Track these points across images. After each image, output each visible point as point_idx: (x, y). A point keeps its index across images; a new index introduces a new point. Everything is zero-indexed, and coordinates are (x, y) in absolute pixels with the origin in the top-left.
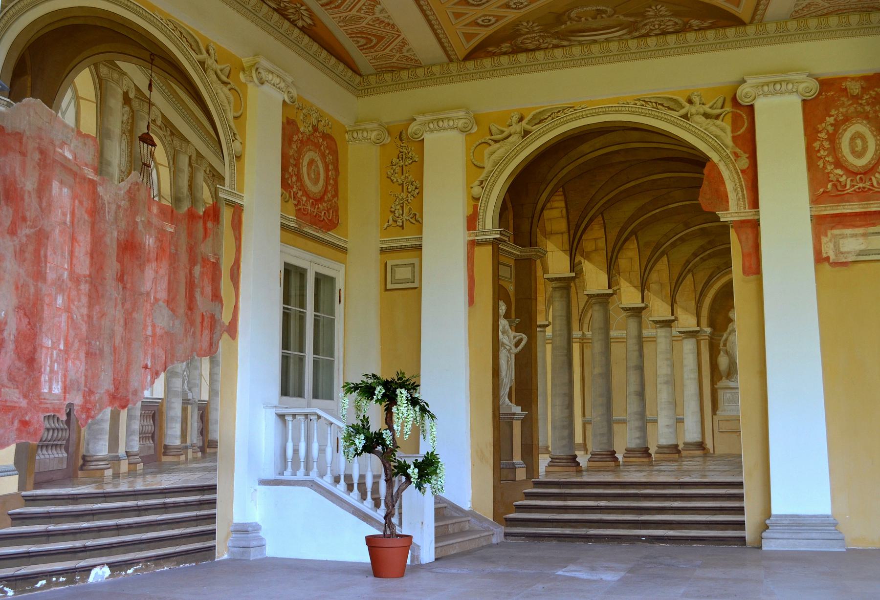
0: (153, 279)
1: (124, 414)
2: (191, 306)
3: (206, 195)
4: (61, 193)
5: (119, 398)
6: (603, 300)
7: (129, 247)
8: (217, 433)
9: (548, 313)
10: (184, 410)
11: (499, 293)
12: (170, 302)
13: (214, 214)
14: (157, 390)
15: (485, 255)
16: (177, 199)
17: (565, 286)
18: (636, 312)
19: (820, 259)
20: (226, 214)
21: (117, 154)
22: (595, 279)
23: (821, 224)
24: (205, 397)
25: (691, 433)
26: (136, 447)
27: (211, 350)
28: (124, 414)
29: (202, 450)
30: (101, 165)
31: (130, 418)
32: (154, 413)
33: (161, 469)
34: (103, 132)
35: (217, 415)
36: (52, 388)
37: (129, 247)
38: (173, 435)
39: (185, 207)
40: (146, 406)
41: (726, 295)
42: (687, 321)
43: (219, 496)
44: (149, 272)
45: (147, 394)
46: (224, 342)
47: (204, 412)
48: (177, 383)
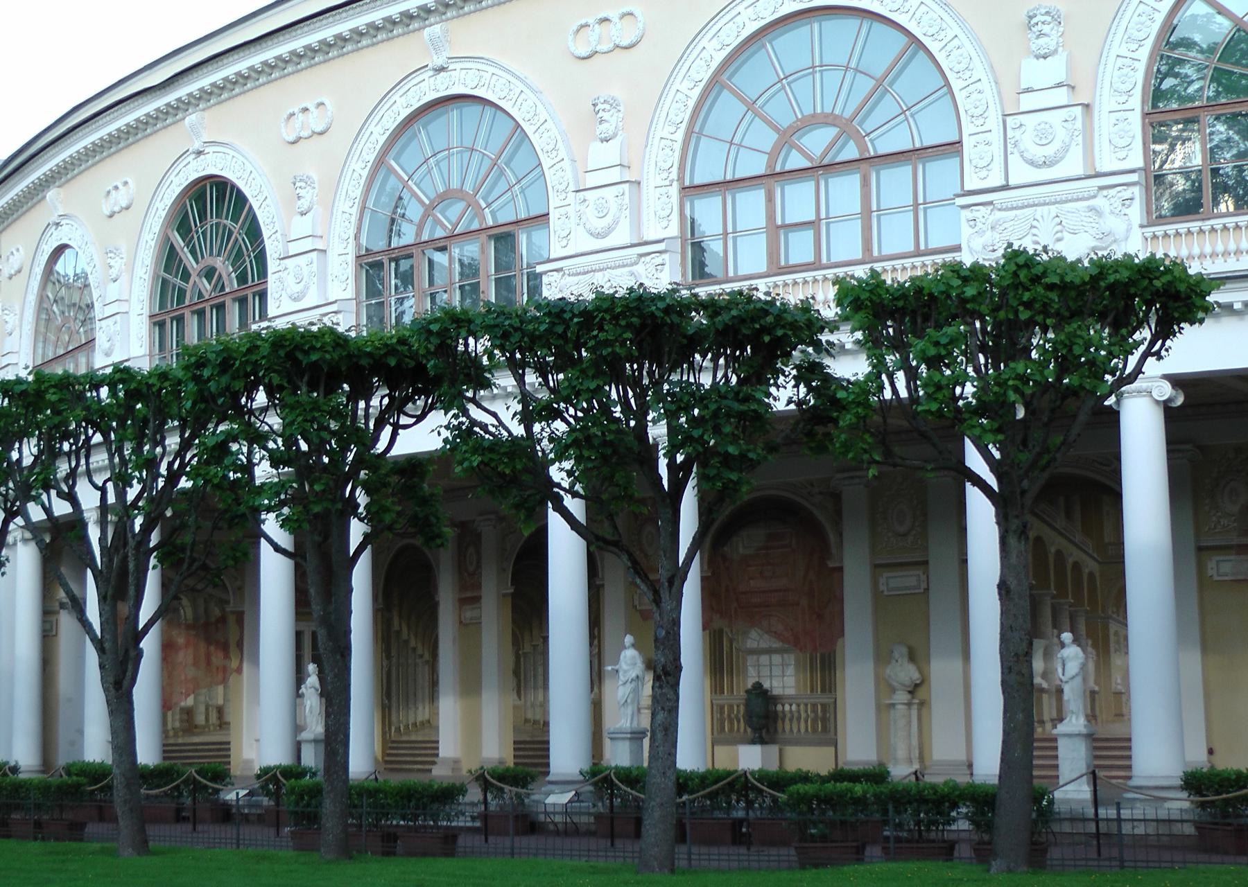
1: (170, 713)
2: (209, 663)
8: (228, 718)
10: (207, 709)
12: (196, 664)
13: (223, 619)
14: (190, 701)
16: (196, 619)
19: (461, 622)
20: (232, 619)
24: (220, 702)
26: (177, 725)
27: (224, 681)
28: (170, 713)
29: (220, 726)
31: (173, 715)
32: (189, 713)
33: (194, 734)
35: (226, 710)
38: (200, 719)
39: (202, 621)
40: (182, 709)
42: (427, 656)
43: (232, 746)
44: (181, 654)
45: (183, 704)
46: (232, 679)
47: (220, 710)
48: (202, 698)
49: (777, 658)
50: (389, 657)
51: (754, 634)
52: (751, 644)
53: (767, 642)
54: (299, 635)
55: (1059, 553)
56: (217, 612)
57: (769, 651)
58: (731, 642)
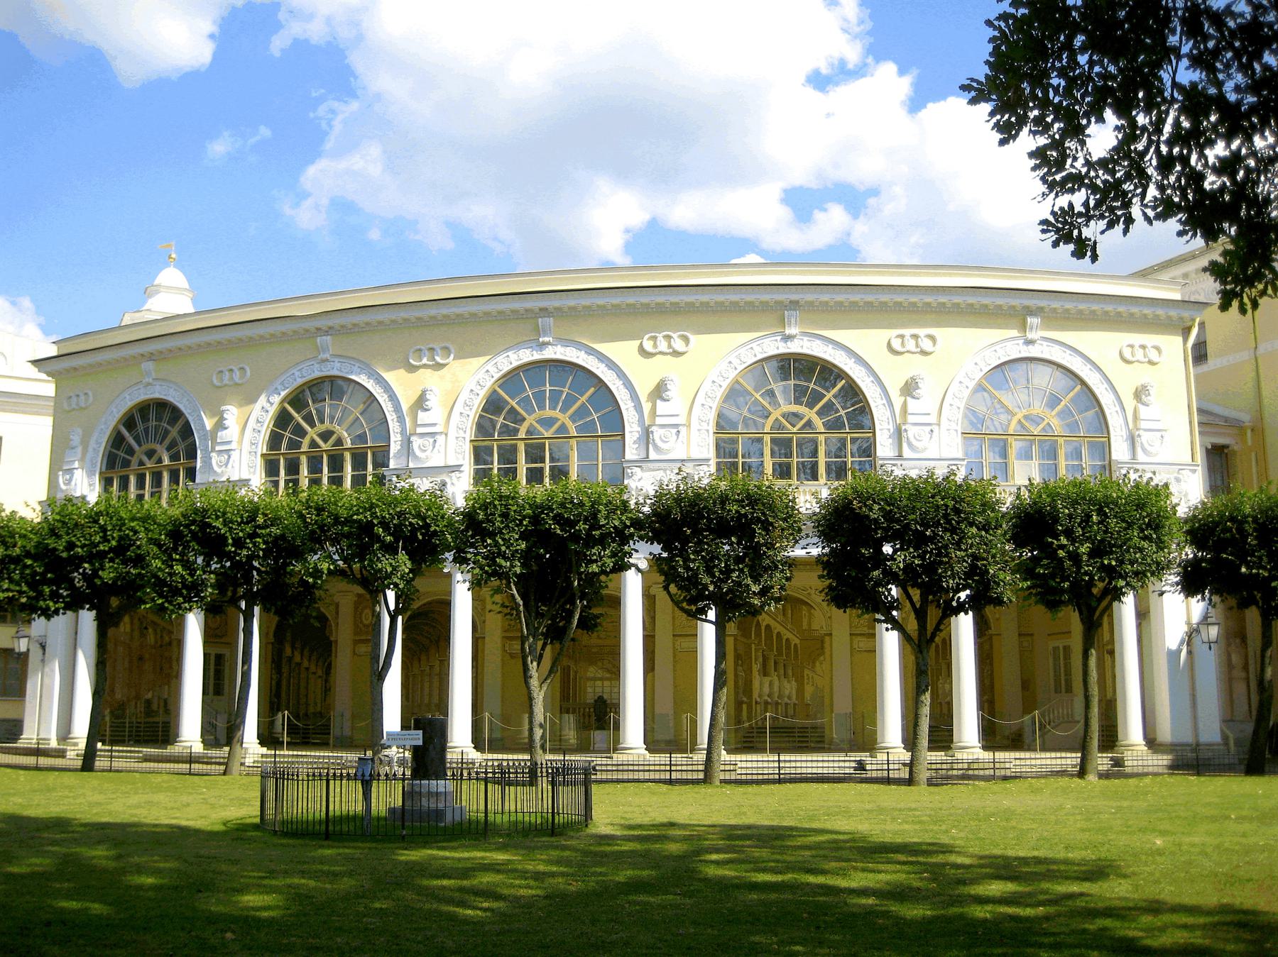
0: (148, 666)
3: (167, 639)
4: (120, 649)
5: (137, 697)
6: (299, 664)
7: (141, 658)
9: (285, 669)
11: (273, 661)
13: (170, 644)
14: (149, 695)
15: (270, 647)
17: (290, 659)
18: (307, 669)
19: (354, 653)
20: (175, 643)
21: (136, 633)
22: (297, 658)
23: (356, 642)
25: (319, 709)
27: (169, 683)
30: (132, 638)
32: (148, 702)
34: (132, 630)
36: (118, 696)
37: (141, 658)
38: (155, 707)
41: (330, 664)
42: (320, 673)
49: (607, 683)
50: (279, 672)
51: (591, 669)
52: (589, 674)
53: (600, 674)
54: (1230, 666)
55: (779, 633)
56: (167, 639)
57: (601, 679)
58: (576, 673)
